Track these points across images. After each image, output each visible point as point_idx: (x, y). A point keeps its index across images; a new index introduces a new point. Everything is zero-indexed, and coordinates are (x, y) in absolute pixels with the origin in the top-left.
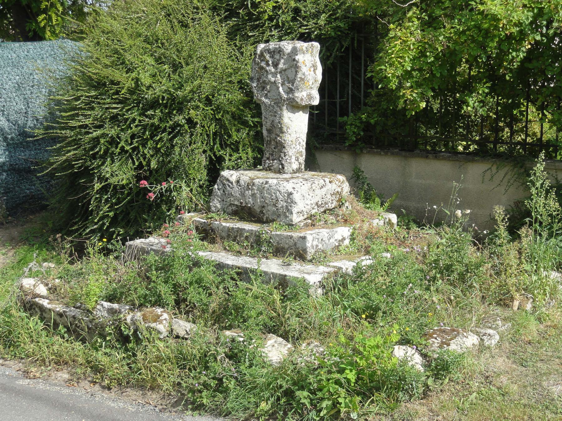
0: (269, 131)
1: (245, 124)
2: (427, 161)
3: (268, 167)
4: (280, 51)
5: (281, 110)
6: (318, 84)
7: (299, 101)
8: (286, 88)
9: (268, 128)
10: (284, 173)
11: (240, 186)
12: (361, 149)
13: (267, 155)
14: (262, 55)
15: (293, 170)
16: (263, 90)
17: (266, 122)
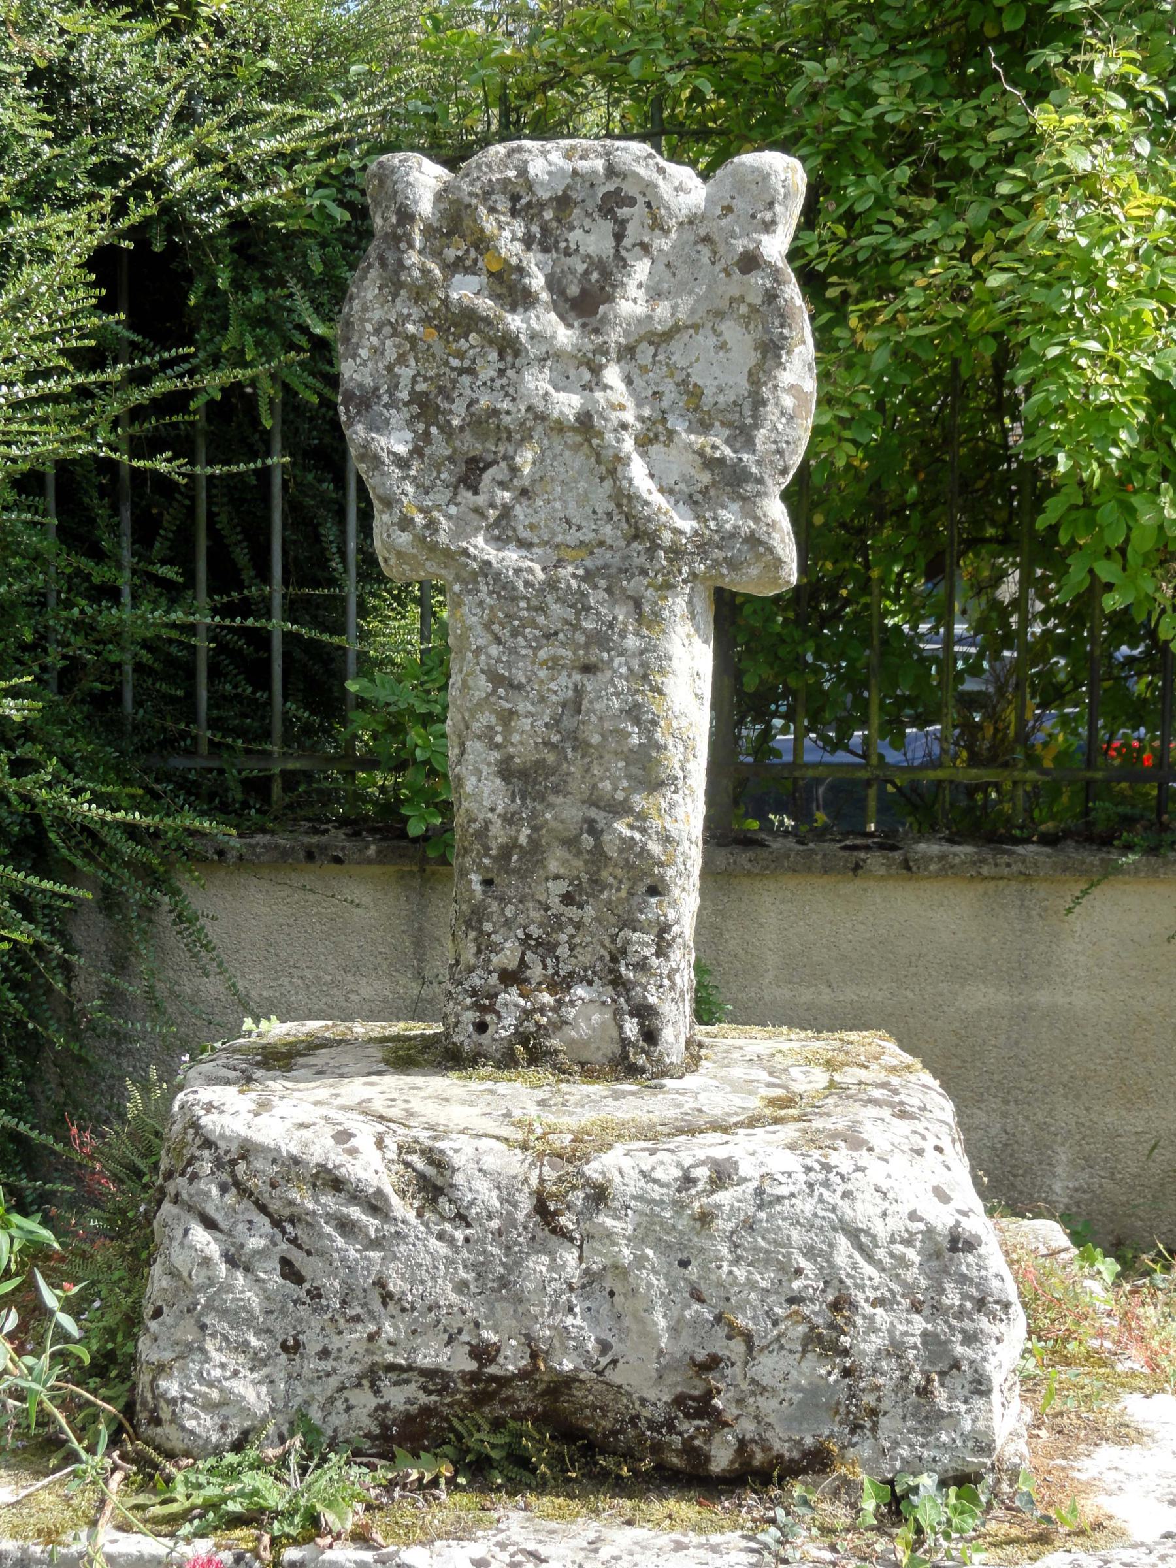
0: (524, 779)
2: (849, 887)
3: (523, 1038)
5: (649, 619)
10: (663, 1074)
11: (462, 1219)
13: (508, 956)
17: (507, 717)
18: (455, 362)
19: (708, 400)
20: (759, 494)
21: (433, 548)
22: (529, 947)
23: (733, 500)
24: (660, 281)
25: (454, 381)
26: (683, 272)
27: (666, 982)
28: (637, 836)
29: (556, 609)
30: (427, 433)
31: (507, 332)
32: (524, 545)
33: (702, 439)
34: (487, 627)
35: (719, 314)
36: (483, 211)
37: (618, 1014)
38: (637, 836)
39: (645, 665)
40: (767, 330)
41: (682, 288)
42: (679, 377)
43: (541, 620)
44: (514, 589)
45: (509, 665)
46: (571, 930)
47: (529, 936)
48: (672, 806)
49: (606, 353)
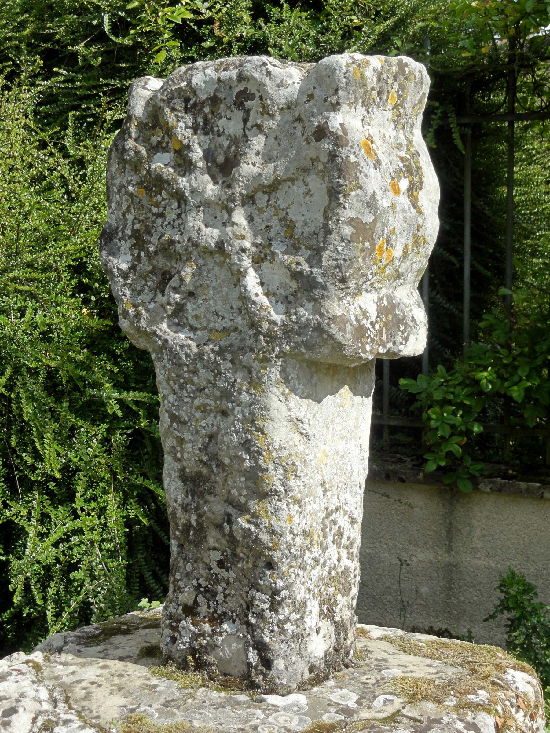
0: (195, 483)
1: (94, 411)
3: (193, 651)
4: (244, 96)
5: (255, 382)
6: (421, 261)
7: (346, 337)
8: (279, 277)
9: (191, 467)
12: (474, 481)
13: (187, 596)
14: (155, 120)
15: (312, 669)
16: (161, 288)
17: (181, 441)
18: (155, 210)
19: (298, 231)
20: (323, 297)
21: (138, 329)
22: (201, 592)
23: (309, 301)
24: (272, 149)
25: (153, 222)
26: (285, 143)
27: (276, 628)
28: (253, 528)
29: (203, 372)
30: (139, 256)
31: (178, 189)
32: (193, 329)
33: (291, 258)
34: (168, 381)
35: (306, 170)
36: (167, 110)
37: (247, 645)
38: (253, 528)
39: (252, 413)
40: (330, 181)
41: (284, 153)
42: (282, 215)
43: (195, 379)
44: (180, 358)
45: (178, 408)
46: (224, 584)
47: (200, 585)
48: (277, 510)
49: (234, 201)
